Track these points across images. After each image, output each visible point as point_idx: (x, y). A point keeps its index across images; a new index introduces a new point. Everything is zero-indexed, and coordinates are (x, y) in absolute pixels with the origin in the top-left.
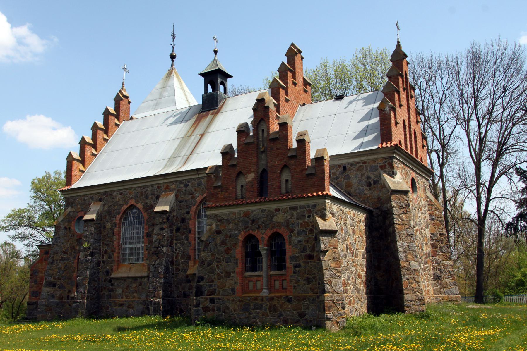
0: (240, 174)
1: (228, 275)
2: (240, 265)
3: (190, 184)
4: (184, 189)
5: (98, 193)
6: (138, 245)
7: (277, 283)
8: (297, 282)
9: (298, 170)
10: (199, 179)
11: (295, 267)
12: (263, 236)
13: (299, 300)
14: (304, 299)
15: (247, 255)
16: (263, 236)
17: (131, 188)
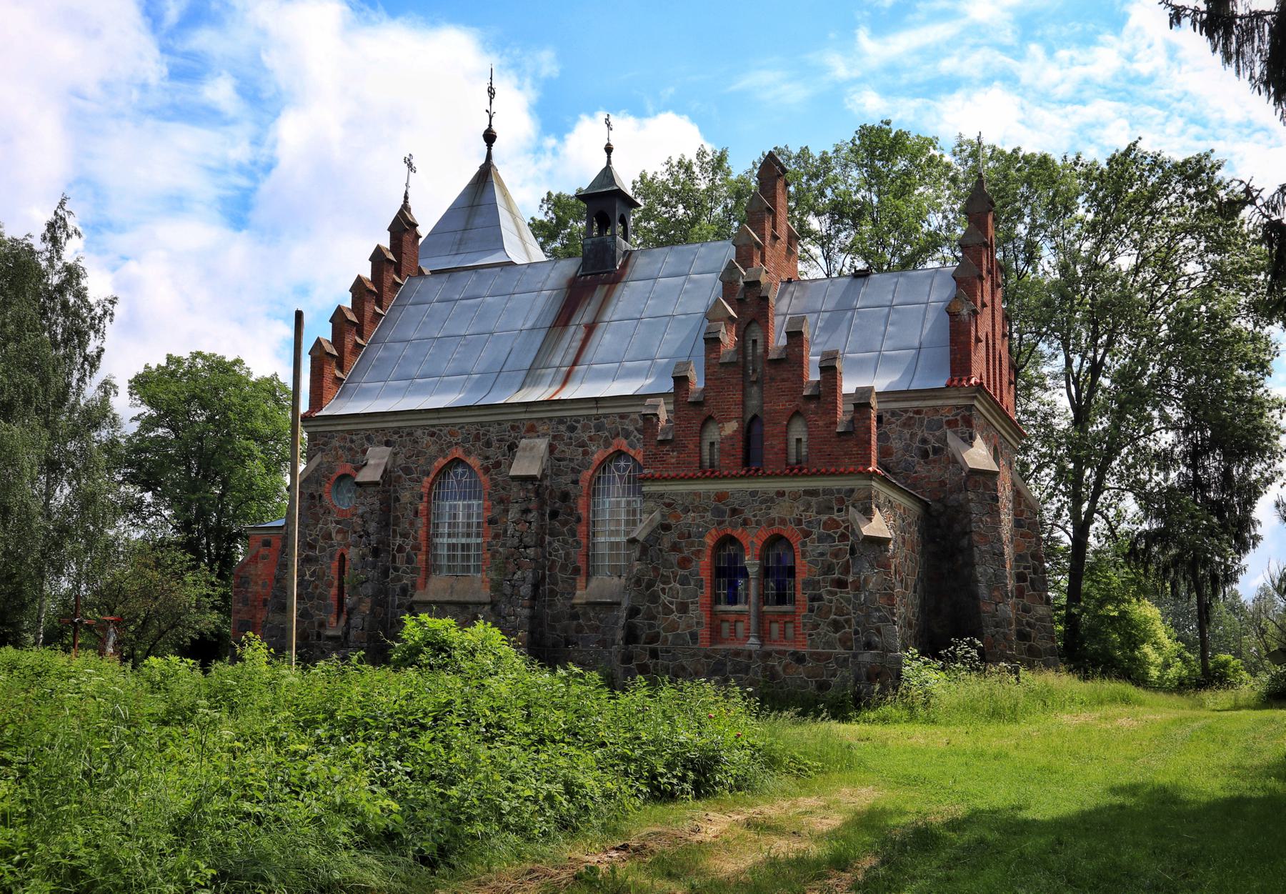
0: (709, 419)
1: (683, 608)
2: (707, 591)
3: (579, 426)
4: (568, 434)
5: (383, 429)
6: (464, 541)
7: (775, 627)
8: (816, 626)
9: (821, 423)
10: (598, 417)
11: (813, 599)
12: (752, 539)
13: (818, 660)
14: (829, 656)
15: (719, 572)
16: (752, 539)
17: (454, 425)
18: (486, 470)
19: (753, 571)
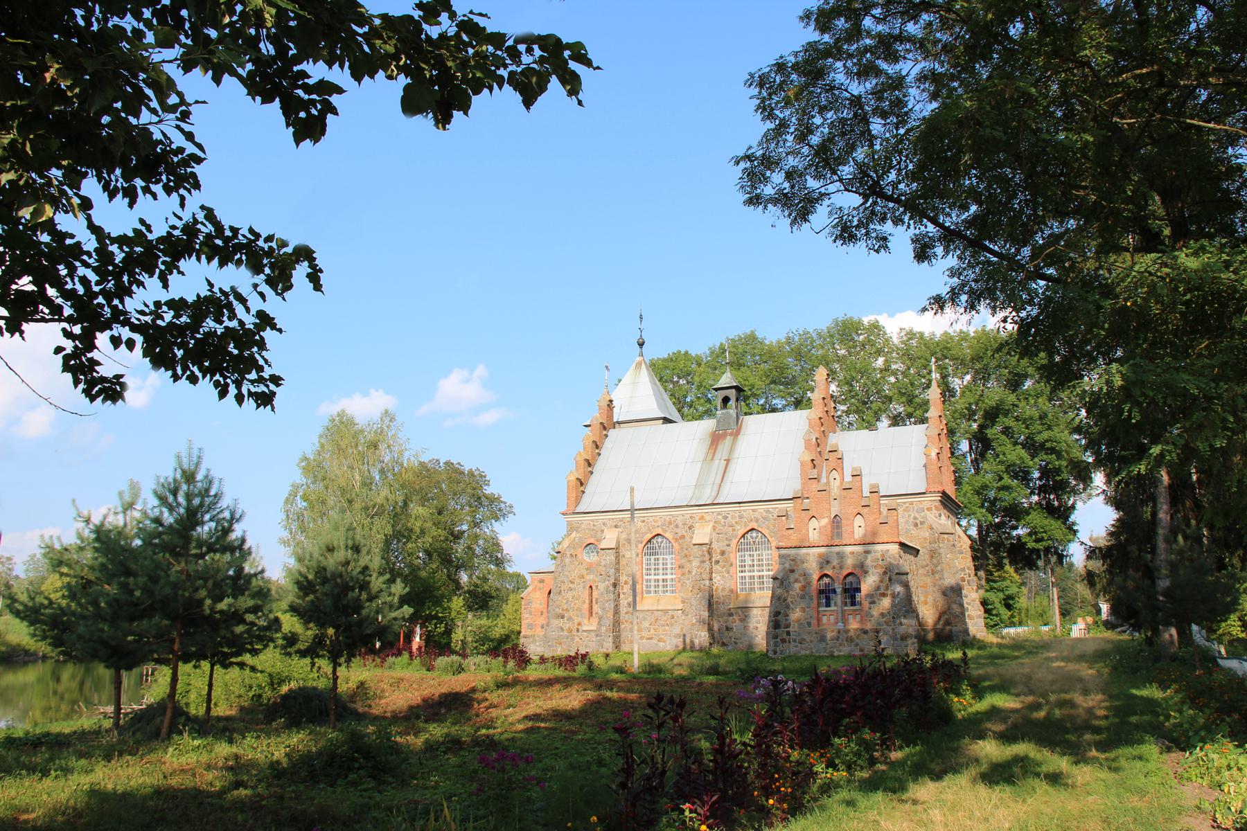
2: (815, 601)
18: (676, 540)
19: (839, 590)
